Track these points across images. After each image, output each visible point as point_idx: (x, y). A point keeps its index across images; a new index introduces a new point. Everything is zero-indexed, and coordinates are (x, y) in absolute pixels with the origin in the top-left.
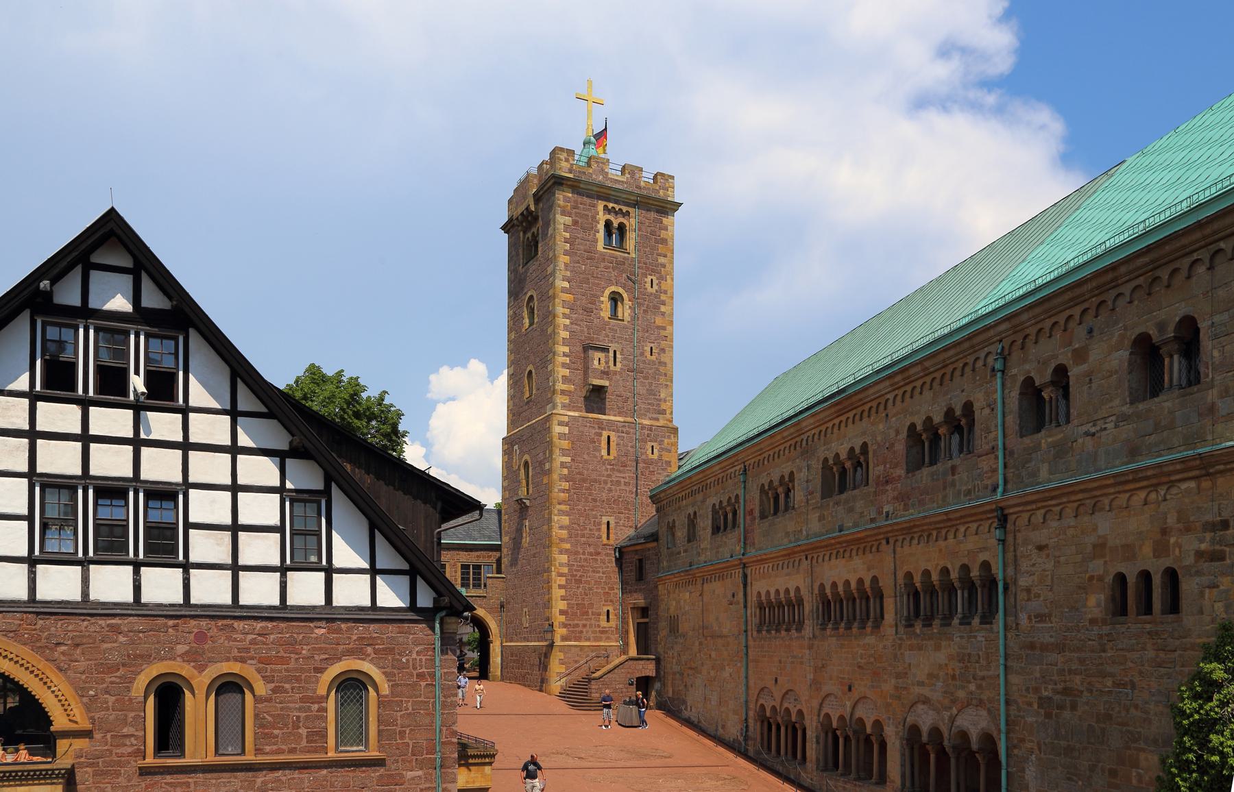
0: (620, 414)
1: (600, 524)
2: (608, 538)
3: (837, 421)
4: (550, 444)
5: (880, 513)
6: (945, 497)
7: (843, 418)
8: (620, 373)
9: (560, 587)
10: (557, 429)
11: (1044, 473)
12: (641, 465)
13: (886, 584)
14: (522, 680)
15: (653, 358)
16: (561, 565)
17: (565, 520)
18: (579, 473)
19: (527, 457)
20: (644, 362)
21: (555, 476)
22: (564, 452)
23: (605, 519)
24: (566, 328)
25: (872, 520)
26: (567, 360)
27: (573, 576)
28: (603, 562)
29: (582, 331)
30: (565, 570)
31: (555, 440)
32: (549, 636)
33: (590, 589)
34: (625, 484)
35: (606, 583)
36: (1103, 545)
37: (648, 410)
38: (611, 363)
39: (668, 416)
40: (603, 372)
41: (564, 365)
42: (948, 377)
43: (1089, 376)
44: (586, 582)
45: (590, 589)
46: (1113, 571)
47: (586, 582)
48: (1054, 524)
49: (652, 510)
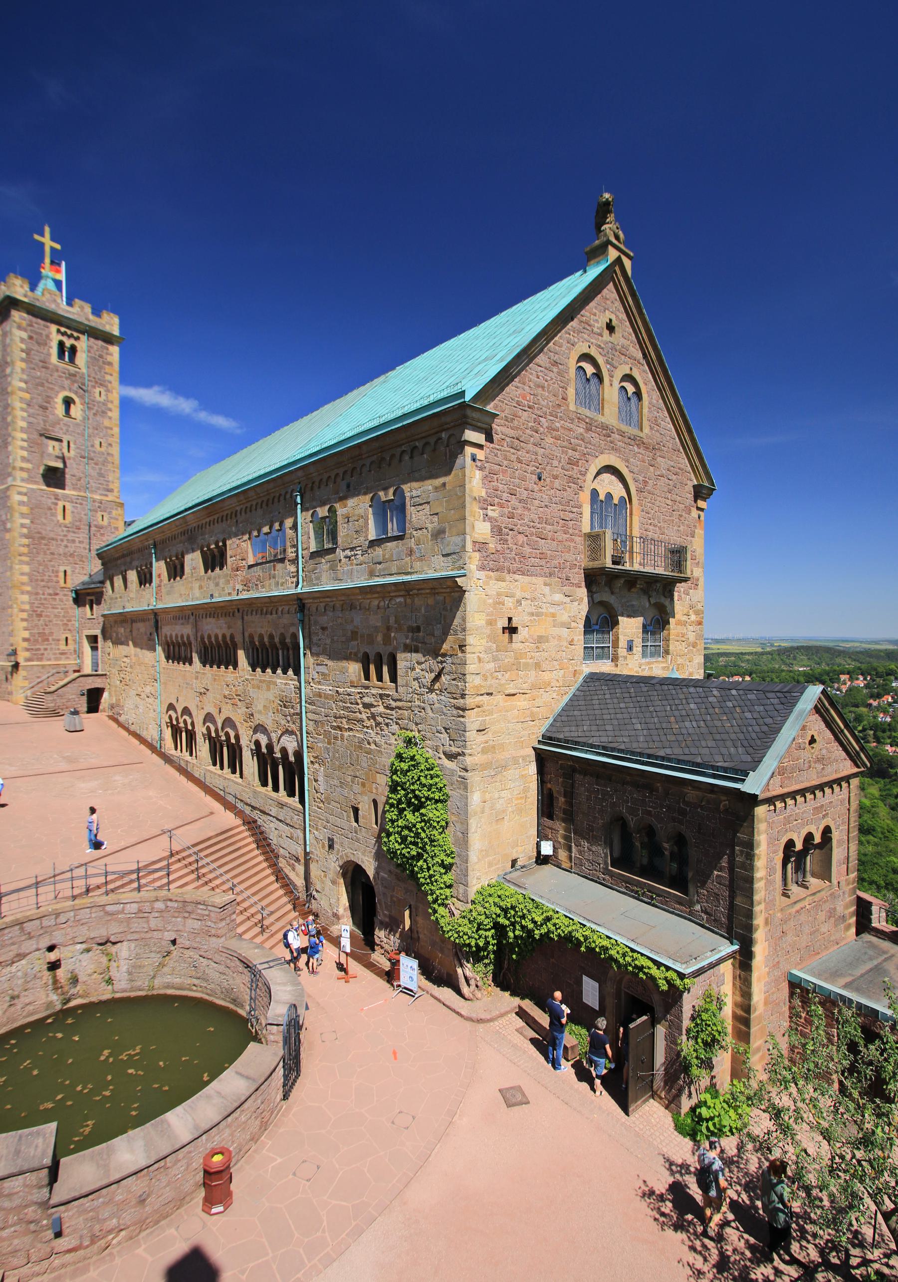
0: (74, 489)
1: (57, 572)
2: (65, 582)
3: (208, 520)
4: (10, 509)
5: (234, 589)
6: (270, 585)
7: (211, 518)
8: (74, 459)
9: (23, 620)
10: (17, 498)
11: (324, 577)
12: (93, 529)
13: (238, 639)
15: (103, 449)
16: (23, 603)
17: (26, 569)
18: (39, 533)
20: (94, 452)
21: (16, 534)
22: (23, 515)
23: (62, 569)
25: (230, 594)
26: (25, 444)
28: (61, 600)
29: (38, 423)
30: (27, 607)
31: (16, 506)
32: (13, 658)
33: (50, 621)
34: (80, 542)
35: (64, 617)
36: (357, 632)
37: (99, 488)
38: (65, 450)
39: (116, 493)
40: (58, 457)
41: (22, 448)
43: (348, 519)
44: (47, 616)
46: (362, 651)
47: (47, 616)
48: (331, 614)
49: (96, 566)
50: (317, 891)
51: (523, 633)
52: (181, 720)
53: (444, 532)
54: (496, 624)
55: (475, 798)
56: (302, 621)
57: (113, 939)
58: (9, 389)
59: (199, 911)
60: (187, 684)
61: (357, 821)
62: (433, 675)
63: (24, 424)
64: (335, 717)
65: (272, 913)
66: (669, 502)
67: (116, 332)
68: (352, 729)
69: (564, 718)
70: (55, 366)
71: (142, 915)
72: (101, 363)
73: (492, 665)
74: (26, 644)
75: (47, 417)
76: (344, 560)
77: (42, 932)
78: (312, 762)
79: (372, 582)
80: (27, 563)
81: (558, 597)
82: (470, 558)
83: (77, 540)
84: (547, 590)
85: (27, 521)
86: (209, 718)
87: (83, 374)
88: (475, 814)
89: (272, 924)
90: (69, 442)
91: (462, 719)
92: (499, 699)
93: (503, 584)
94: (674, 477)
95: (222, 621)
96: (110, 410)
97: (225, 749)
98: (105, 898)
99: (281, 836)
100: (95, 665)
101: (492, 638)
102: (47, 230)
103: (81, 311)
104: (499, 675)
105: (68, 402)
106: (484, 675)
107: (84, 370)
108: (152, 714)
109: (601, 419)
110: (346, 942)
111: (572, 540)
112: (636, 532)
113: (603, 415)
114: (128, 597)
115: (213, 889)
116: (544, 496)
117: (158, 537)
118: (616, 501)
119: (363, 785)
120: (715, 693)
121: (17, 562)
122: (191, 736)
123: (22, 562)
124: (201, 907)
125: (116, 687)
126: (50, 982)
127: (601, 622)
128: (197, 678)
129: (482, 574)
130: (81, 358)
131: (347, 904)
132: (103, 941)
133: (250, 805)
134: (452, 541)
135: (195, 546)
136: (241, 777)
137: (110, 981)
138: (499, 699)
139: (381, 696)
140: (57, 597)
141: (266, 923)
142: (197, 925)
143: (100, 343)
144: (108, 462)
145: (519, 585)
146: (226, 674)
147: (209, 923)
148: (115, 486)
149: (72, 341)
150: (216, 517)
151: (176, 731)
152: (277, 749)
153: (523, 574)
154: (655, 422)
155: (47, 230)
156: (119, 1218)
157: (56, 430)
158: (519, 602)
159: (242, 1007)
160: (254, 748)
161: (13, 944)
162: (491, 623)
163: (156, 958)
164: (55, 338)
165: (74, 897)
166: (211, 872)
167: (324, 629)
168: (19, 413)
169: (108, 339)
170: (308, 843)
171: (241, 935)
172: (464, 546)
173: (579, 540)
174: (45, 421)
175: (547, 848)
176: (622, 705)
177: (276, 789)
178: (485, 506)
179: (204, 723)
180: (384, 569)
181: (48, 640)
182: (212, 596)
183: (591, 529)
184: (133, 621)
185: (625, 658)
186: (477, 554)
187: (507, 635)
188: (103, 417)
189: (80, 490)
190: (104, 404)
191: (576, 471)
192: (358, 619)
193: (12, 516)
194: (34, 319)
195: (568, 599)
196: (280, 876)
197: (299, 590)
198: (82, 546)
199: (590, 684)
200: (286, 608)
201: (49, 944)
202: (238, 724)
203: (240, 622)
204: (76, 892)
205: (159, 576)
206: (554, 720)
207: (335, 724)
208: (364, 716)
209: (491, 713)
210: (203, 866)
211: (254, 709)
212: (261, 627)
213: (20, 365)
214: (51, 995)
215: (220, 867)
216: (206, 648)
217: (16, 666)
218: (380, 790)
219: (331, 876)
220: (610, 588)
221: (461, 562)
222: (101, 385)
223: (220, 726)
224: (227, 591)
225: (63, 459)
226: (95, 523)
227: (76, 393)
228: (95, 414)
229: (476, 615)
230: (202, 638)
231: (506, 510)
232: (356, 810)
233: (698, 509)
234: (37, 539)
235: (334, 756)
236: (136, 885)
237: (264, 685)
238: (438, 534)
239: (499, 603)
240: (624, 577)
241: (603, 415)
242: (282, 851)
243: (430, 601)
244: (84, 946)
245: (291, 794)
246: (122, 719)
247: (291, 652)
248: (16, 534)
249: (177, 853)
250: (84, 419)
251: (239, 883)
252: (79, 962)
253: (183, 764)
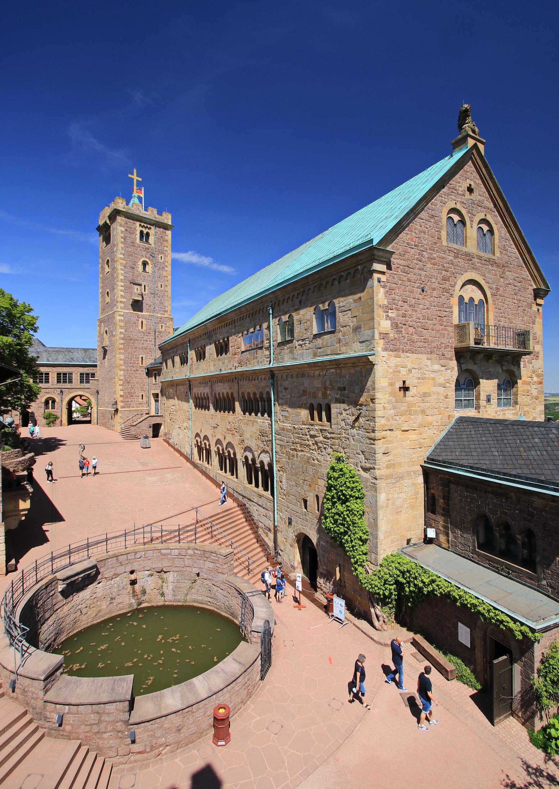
1: (138, 358)
3: (219, 326)
4: (115, 324)
6: (254, 363)
7: (221, 325)
9: (120, 385)
10: (119, 318)
11: (286, 358)
12: (157, 333)
13: (236, 395)
14: (105, 425)
16: (120, 376)
17: (122, 357)
19: (106, 328)
23: (141, 356)
25: (231, 369)
26: (123, 288)
28: (140, 374)
29: (130, 276)
30: (123, 378)
31: (118, 323)
33: (134, 386)
34: (150, 341)
36: (306, 391)
38: (143, 290)
39: (169, 313)
40: (139, 294)
41: (121, 291)
42: (254, 313)
43: (300, 322)
44: (132, 383)
45: (134, 386)
46: (309, 402)
48: (290, 380)
49: (158, 354)
50: (281, 550)
51: (413, 391)
52: (203, 443)
53: (360, 328)
54: (395, 385)
55: (382, 497)
56: (273, 384)
57: (165, 570)
58: (115, 259)
59: (213, 557)
60: (207, 422)
61: (306, 508)
62: (354, 418)
63: (122, 278)
64: (293, 443)
65: (254, 562)
66: (515, 301)
67: (170, 223)
68: (303, 451)
69: (442, 447)
70: (138, 244)
71: (180, 557)
72: (162, 241)
73: (392, 412)
74: (121, 399)
76: (298, 347)
77: (127, 562)
78: (279, 470)
81: (437, 367)
82: (377, 343)
84: (429, 362)
86: (218, 442)
87: (153, 248)
88: (382, 507)
89: (255, 569)
91: (373, 446)
92: (397, 433)
93: (399, 359)
94: (519, 284)
95: (226, 385)
97: (228, 461)
98: (160, 545)
99: (259, 515)
100: (157, 410)
101: (392, 394)
102: (135, 171)
103: (152, 214)
104: (397, 418)
105: (145, 264)
106: (387, 418)
107: (153, 246)
108: (187, 439)
109: (465, 249)
110: (299, 584)
111: (446, 330)
112: (491, 322)
113: (466, 247)
114: (175, 371)
115: (220, 544)
116: (426, 302)
117: (191, 337)
118: (476, 302)
119: (310, 486)
120: (554, 431)
122: (208, 452)
123: (120, 353)
124: (214, 555)
125: (168, 423)
126: (131, 592)
127: (467, 383)
128: (212, 418)
129: (385, 354)
130: (152, 239)
131: (300, 560)
132: (160, 571)
133: (242, 495)
134: (365, 333)
135: (211, 341)
136: (237, 478)
137: (163, 594)
138: (397, 433)
139: (321, 430)
141: (251, 567)
142: (211, 565)
143: (161, 230)
145: (410, 360)
146: (228, 416)
147: (218, 565)
148: (169, 309)
149: (147, 230)
150: (223, 324)
151: (200, 449)
152: (258, 462)
153: (413, 353)
154: (504, 249)
155: (135, 171)
156: (166, 738)
158: (410, 371)
159: (237, 618)
160: (244, 460)
161: (112, 568)
162: (391, 384)
163: (188, 583)
164: (139, 229)
165: (145, 544)
166: (219, 534)
167: (286, 389)
168: (120, 272)
169: (165, 227)
170: (276, 520)
171: (236, 574)
172: (373, 336)
173: (451, 329)
175: (431, 533)
176: (484, 439)
177: (257, 486)
178: (387, 310)
179: (216, 445)
180: (323, 352)
181: (133, 396)
182: (221, 370)
183: (459, 321)
184: (177, 385)
185: (485, 407)
186: (382, 341)
187: (402, 392)
191: (448, 285)
192: (306, 383)
194: (128, 220)
195: (443, 368)
196: (259, 539)
197: (271, 366)
199: (460, 424)
200: (264, 377)
201: (131, 569)
202: (235, 446)
203: (236, 386)
204: (146, 540)
205: (192, 359)
206: (435, 448)
207: (293, 447)
208: (310, 443)
209: (392, 442)
210: (215, 530)
211: (244, 437)
212: (249, 388)
213: (121, 245)
214: (131, 599)
215: (224, 531)
216: (217, 400)
217: (117, 411)
218: (320, 489)
219: (290, 542)
220: (474, 360)
221: (372, 346)
222: (162, 253)
223: (225, 447)
224: (229, 367)
225: (142, 295)
227: (149, 259)
229: (382, 380)
230: (215, 395)
231: (400, 312)
232: (305, 501)
233: (537, 305)
234: (128, 340)
235: (292, 467)
236: (177, 539)
237: (250, 423)
238: (357, 329)
239: (397, 372)
240: (483, 353)
241: (466, 247)
242: (260, 524)
243: (352, 371)
244: (149, 572)
245: (266, 489)
246: (171, 441)
247: (266, 403)
248: (118, 338)
249: (200, 521)
250: (153, 272)
251: (236, 542)
252: (147, 582)
253: (204, 469)
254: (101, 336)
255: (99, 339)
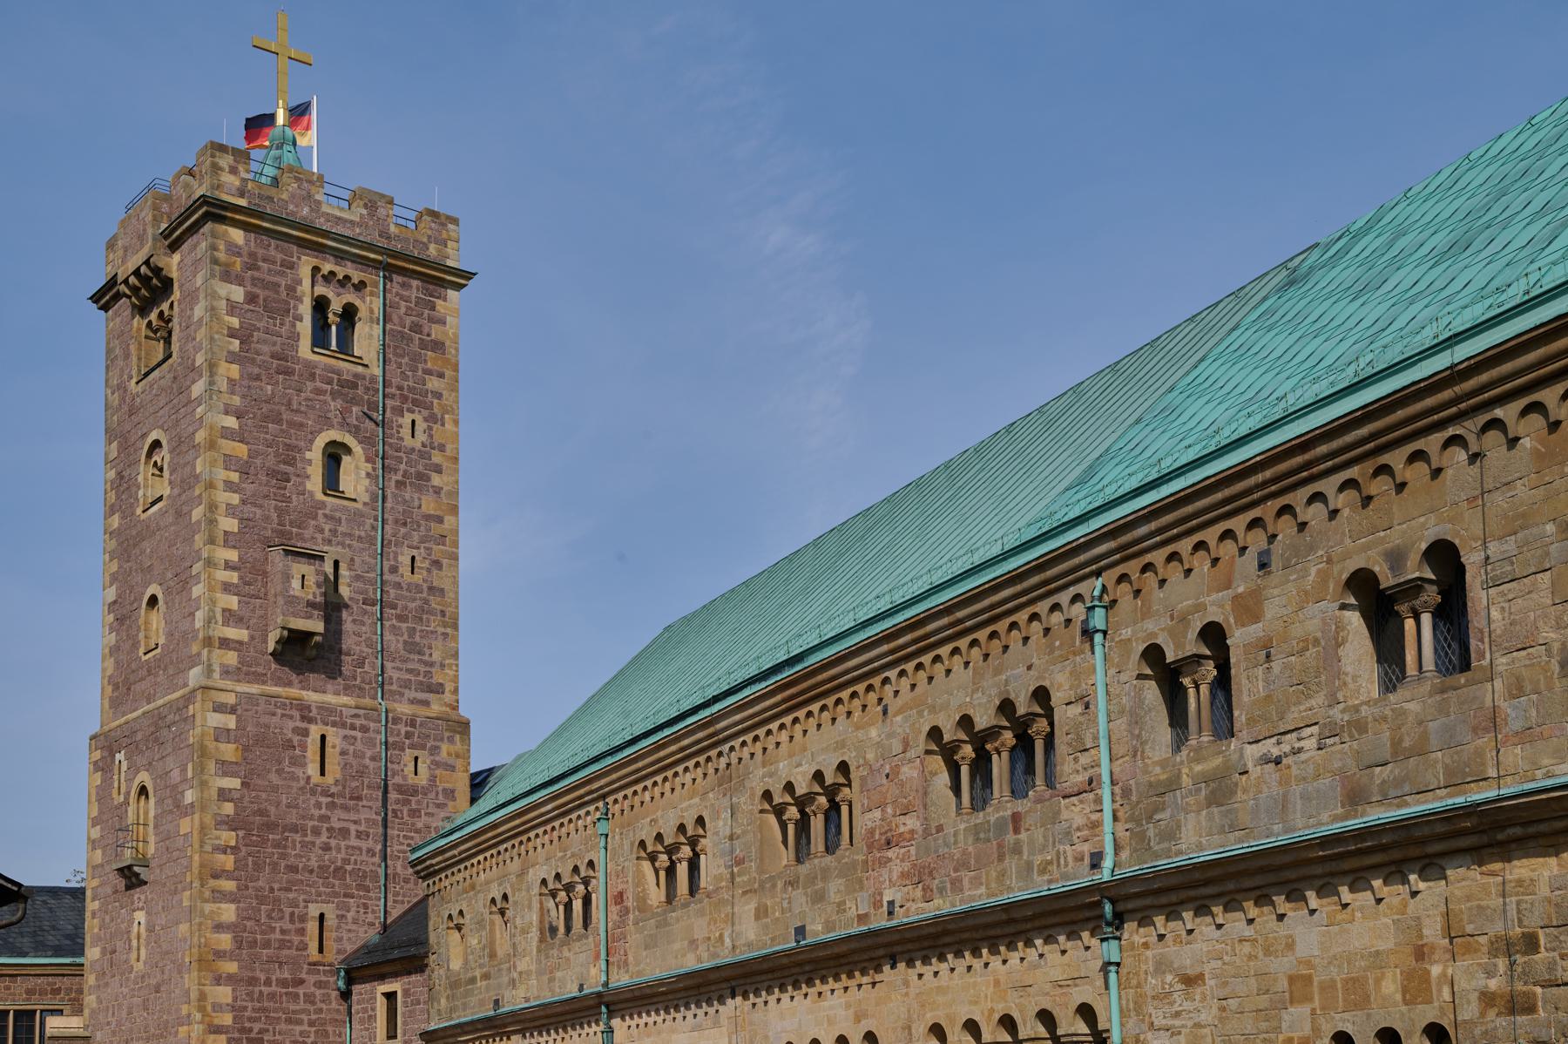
0: (347, 690)
1: (303, 918)
2: (321, 950)
12: (393, 796)
15: (418, 578)
16: (217, 1007)
17: (228, 912)
19: (144, 777)
20: (398, 586)
22: (225, 768)
23: (314, 910)
24: (231, 510)
27: (243, 1030)
30: (227, 1019)
31: (211, 745)
34: (359, 835)
37: (406, 684)
40: (311, 604)
41: (227, 588)
75: (288, 500)
79: (1354, 823)
80: (232, 901)
83: (353, 828)
85: (235, 783)
90: (336, 563)
96: (438, 469)
121: (207, 894)
123: (220, 896)
140: (301, 991)
144: (431, 612)
157: (307, 533)
174: (281, 513)
180: (1398, 782)
188: (419, 489)
189: (361, 691)
190: (422, 455)
193: (201, 769)
198: (364, 845)
222: (415, 402)
226: (398, 780)
227: (355, 431)
228: (400, 484)
234: (258, 829)
248: (208, 819)
250: (374, 498)
254: (109, 817)
255: (96, 833)
